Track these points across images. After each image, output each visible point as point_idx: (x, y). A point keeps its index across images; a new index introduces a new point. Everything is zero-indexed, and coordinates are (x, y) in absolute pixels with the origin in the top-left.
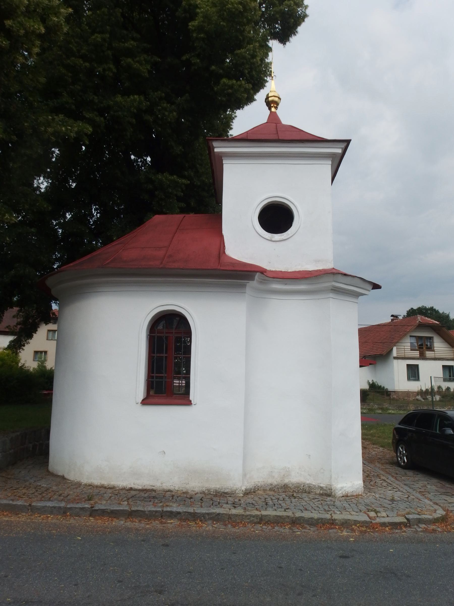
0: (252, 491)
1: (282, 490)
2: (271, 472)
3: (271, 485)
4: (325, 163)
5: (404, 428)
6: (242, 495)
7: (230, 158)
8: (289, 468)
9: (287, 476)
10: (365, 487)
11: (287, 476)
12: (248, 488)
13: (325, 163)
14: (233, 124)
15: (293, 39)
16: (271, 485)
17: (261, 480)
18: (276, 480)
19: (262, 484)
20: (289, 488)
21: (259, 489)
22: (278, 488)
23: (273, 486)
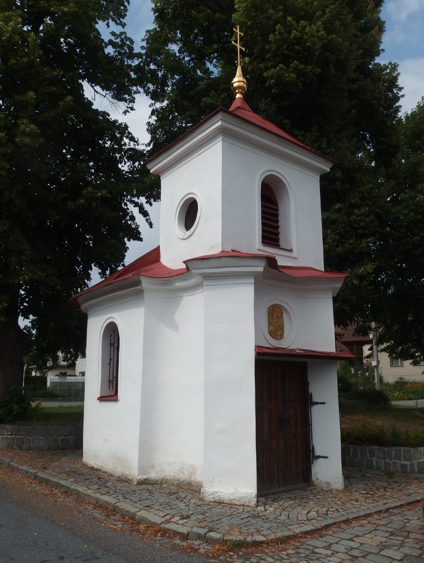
0: (159, 483)
1: (187, 487)
2: (182, 467)
3: (178, 480)
4: (174, 170)
5: (24, 370)
6: (136, 483)
7: (165, 172)
8: (195, 466)
9: (194, 474)
10: (259, 495)
11: (194, 474)
12: (152, 479)
13: (174, 170)
14: (119, 122)
15: (109, 39)
16: (178, 480)
17: (172, 474)
18: (183, 477)
19: (172, 477)
20: (192, 487)
21: (168, 482)
22: (184, 484)
23: (180, 482)
